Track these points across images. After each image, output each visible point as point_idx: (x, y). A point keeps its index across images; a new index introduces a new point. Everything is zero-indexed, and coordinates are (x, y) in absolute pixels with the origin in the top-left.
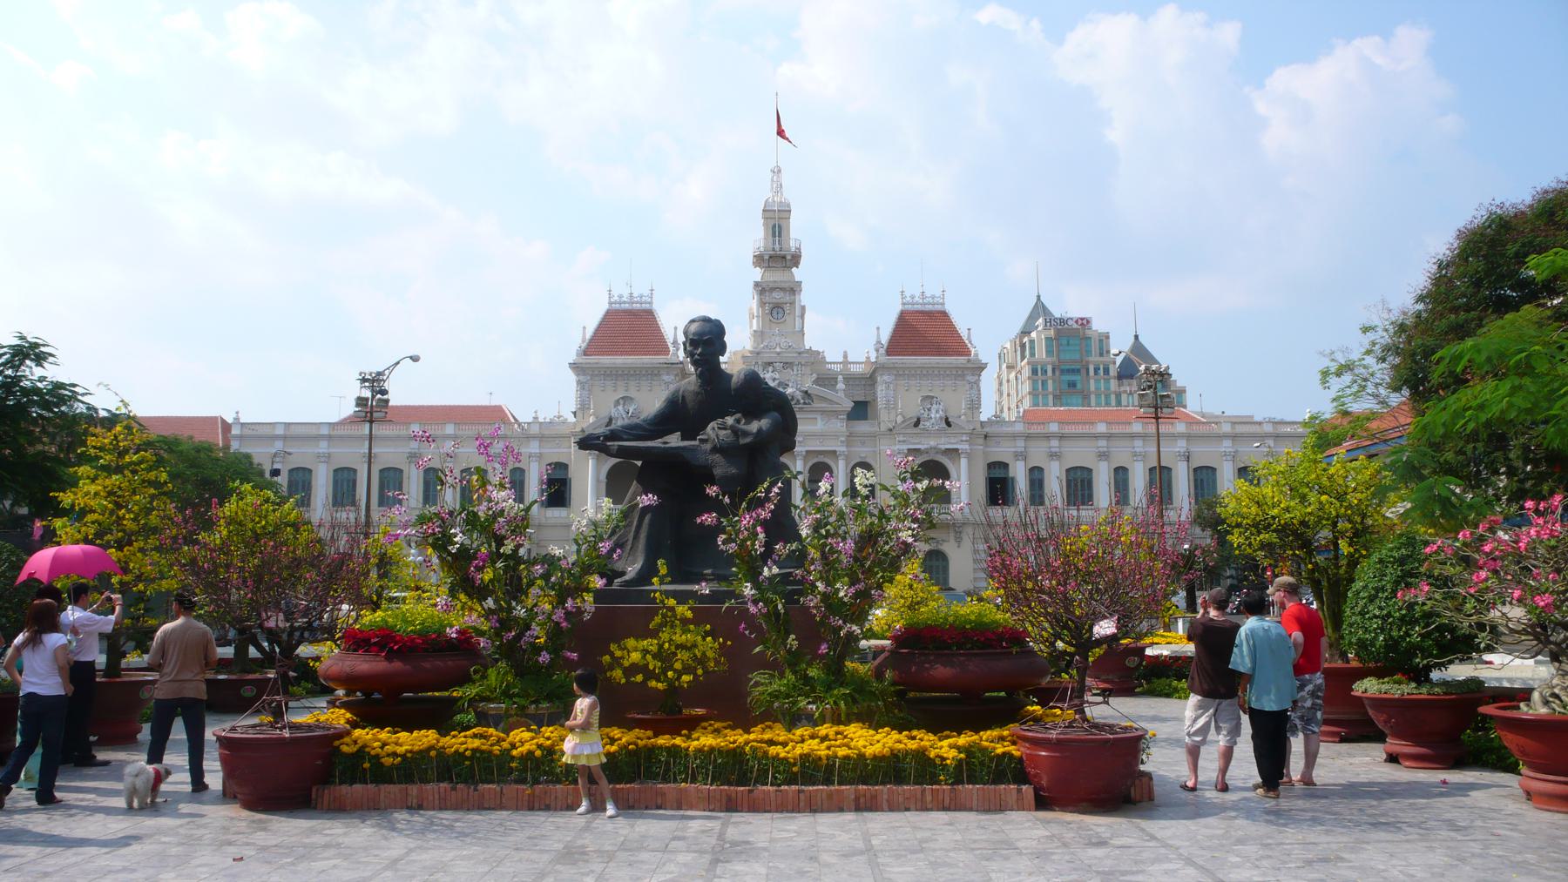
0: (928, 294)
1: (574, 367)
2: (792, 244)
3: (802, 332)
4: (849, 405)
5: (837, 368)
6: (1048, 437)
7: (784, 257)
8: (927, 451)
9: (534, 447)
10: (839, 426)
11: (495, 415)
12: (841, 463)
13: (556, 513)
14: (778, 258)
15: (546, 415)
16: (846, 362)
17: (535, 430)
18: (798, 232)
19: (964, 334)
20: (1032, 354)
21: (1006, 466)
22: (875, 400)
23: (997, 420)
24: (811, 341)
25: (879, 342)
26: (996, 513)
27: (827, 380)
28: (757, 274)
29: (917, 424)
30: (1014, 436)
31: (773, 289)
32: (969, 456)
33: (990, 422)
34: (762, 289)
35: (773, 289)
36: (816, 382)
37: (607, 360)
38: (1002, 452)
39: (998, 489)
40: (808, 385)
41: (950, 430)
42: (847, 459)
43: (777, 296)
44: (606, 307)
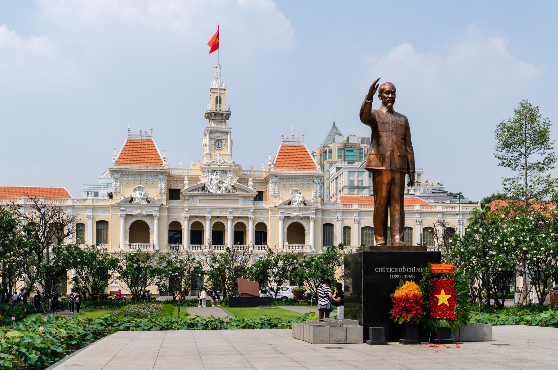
4: (255, 194)
7: (222, 114)
8: (293, 218)
9: (89, 212)
10: (251, 204)
12: (251, 223)
20: (330, 157)
29: (290, 203)
32: (315, 221)
35: (216, 132)
36: (237, 181)
37: (129, 167)
42: (254, 221)
43: (218, 136)
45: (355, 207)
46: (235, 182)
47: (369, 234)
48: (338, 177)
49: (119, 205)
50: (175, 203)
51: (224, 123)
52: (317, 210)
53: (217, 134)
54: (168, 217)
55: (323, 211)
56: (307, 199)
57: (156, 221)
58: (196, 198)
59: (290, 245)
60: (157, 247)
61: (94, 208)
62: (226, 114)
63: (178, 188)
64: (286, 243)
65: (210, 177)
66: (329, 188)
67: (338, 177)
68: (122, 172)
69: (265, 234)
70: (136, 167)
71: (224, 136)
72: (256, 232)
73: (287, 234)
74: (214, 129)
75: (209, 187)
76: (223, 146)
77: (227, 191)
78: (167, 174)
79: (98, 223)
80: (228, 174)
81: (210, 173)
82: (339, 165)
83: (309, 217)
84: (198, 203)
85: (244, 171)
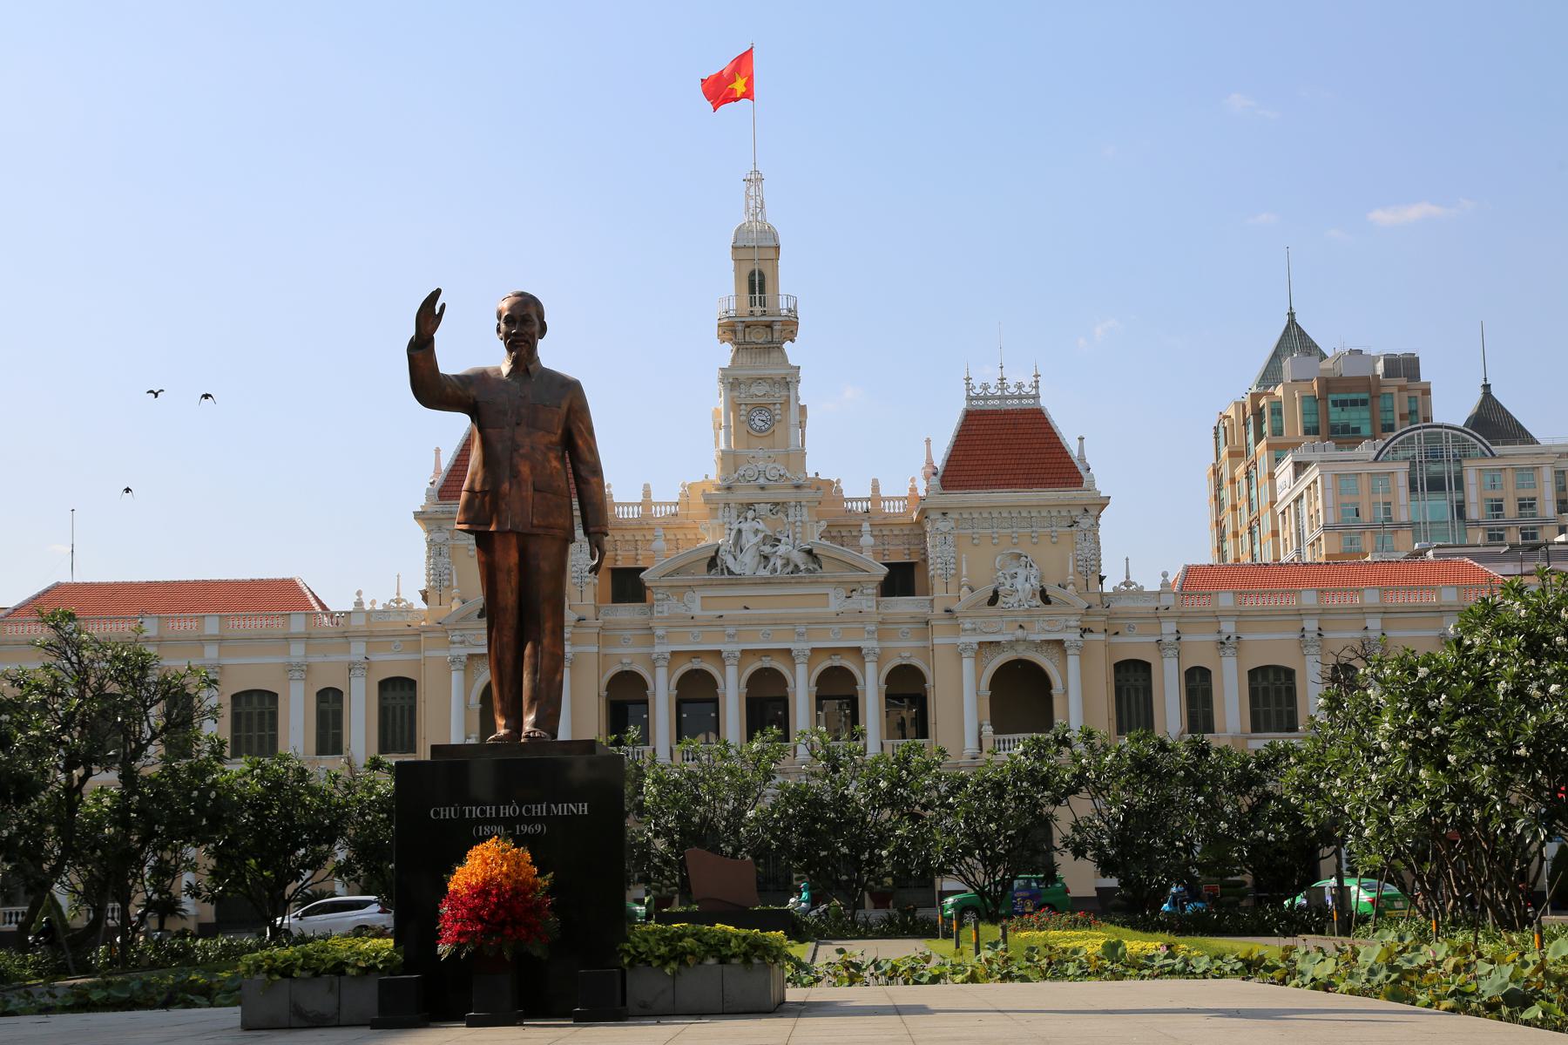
0: (1011, 381)
2: (783, 304)
3: (802, 454)
5: (860, 507)
8: (1012, 644)
12: (871, 668)
15: (378, 597)
16: (876, 497)
17: (358, 622)
19: (1072, 447)
20: (1278, 432)
22: (925, 561)
23: (1129, 590)
24: (817, 464)
25: (930, 463)
27: (843, 528)
28: (725, 353)
29: (993, 600)
32: (1083, 651)
33: (1117, 592)
34: (732, 382)
38: (1135, 645)
40: (813, 537)
41: (1048, 607)
42: (880, 661)
46: (817, 537)
47: (1278, 691)
48: (1301, 496)
50: (627, 613)
51: (775, 355)
53: (755, 390)
54: (603, 658)
58: (689, 594)
59: (1001, 737)
62: (784, 323)
63: (640, 564)
64: (988, 730)
65: (736, 526)
66: (1275, 534)
67: (1301, 496)
69: (920, 702)
71: (779, 393)
72: (887, 696)
73: (992, 698)
76: (777, 427)
77: (790, 569)
79: (385, 685)
80: (791, 511)
81: (734, 513)
82: (1302, 454)
85: (852, 500)
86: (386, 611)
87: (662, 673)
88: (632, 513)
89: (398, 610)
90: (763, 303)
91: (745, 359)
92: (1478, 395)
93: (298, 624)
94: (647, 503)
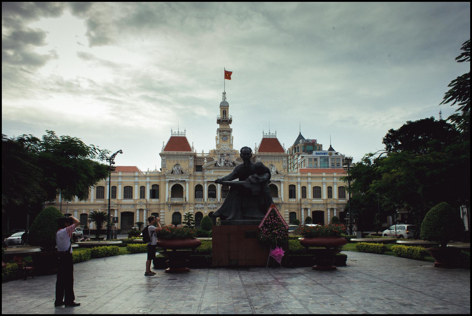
0: (271, 133)
1: (161, 155)
2: (229, 117)
3: (232, 145)
6: (307, 177)
7: (227, 121)
9: (148, 179)
11: (134, 169)
13: (154, 201)
14: (224, 121)
15: (152, 169)
17: (148, 174)
18: (231, 113)
19: (282, 144)
20: (298, 151)
21: (295, 186)
25: (256, 148)
26: (293, 200)
28: (218, 126)
30: (297, 177)
31: (223, 131)
34: (219, 131)
35: (223, 131)
36: (237, 160)
37: (171, 152)
38: (293, 182)
39: (292, 194)
44: (170, 136)
45: (309, 174)
49: (164, 176)
50: (199, 173)
52: (285, 176)
54: (194, 182)
55: (289, 177)
56: (278, 170)
57: (187, 185)
60: (187, 200)
61: (150, 177)
68: (167, 155)
70: (175, 152)
74: (221, 130)
75: (219, 164)
78: (195, 156)
79: (153, 186)
83: (280, 181)
84: (212, 173)
86: (154, 172)
87: (206, 185)
88: (200, 155)
89: (156, 172)
90: (226, 116)
91: (222, 127)
92: (329, 147)
93: (137, 174)
94: (203, 154)
